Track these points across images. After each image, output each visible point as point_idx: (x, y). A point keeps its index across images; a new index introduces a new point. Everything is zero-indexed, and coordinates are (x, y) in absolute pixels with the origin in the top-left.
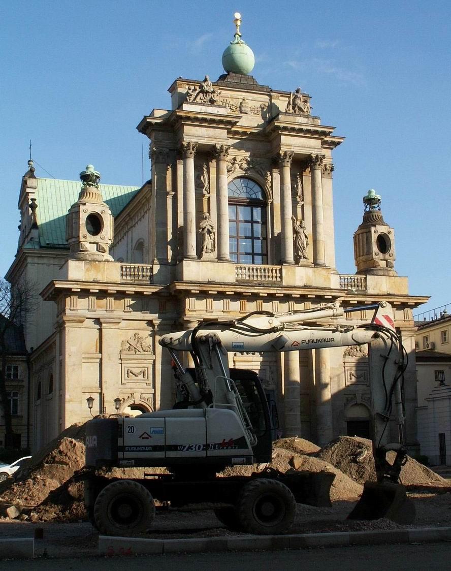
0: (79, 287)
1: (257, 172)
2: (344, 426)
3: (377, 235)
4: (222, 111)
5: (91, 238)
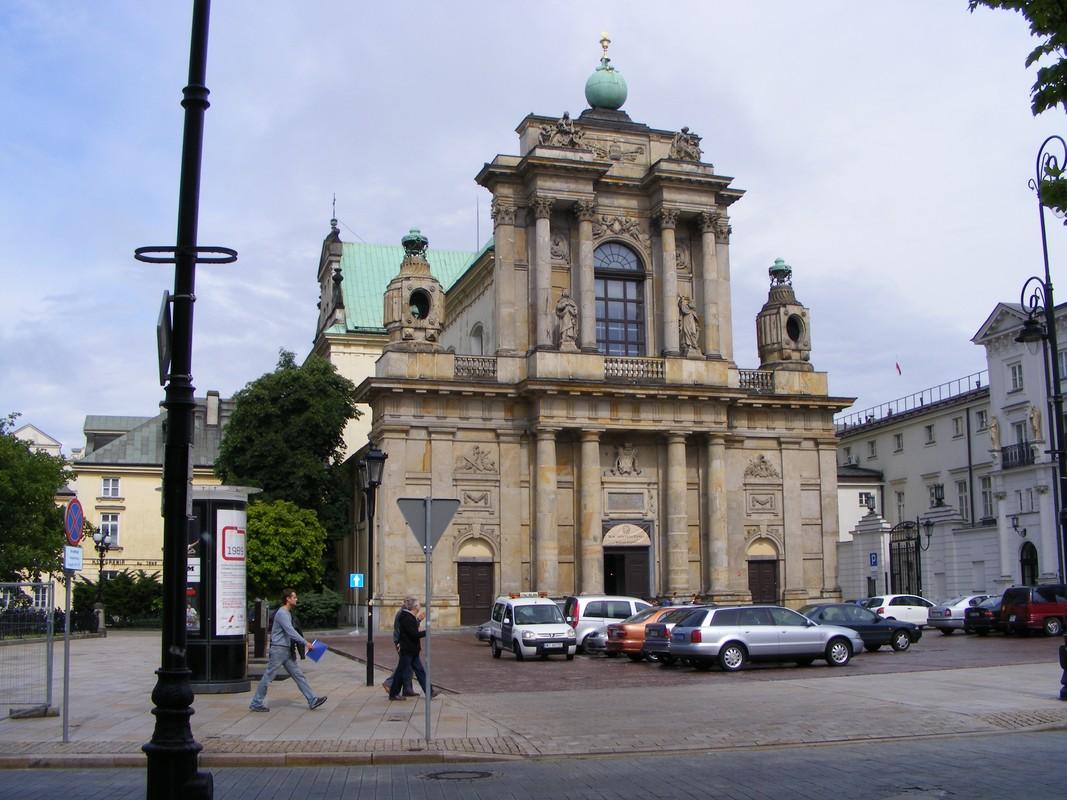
0: (401, 386)
1: (632, 235)
3: (786, 318)
4: (587, 157)
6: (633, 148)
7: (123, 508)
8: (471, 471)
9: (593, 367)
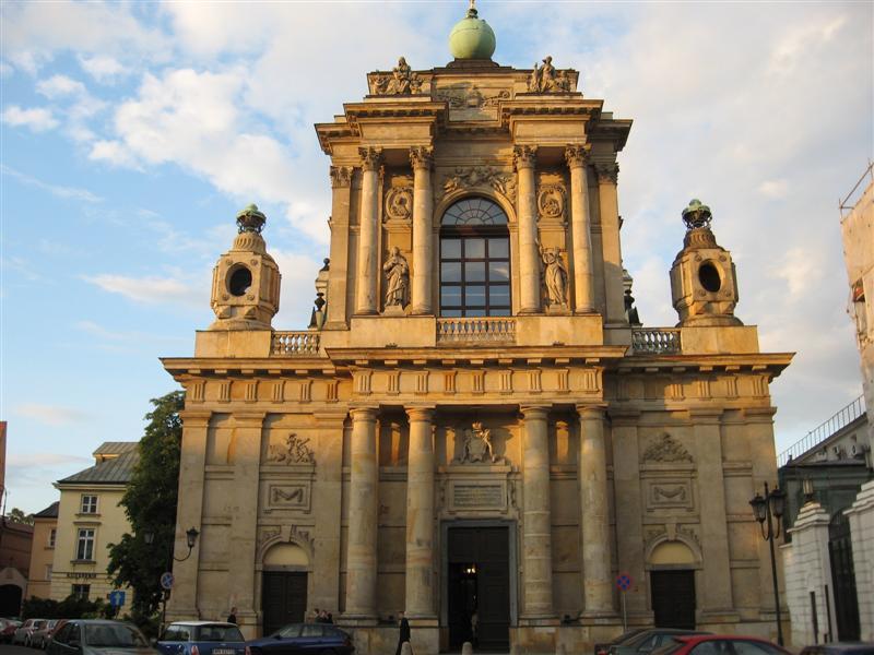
0: (198, 367)
2: (643, 579)
5: (233, 300)
6: (496, 92)
7: (99, 524)
8: (284, 462)
9: (418, 333)
